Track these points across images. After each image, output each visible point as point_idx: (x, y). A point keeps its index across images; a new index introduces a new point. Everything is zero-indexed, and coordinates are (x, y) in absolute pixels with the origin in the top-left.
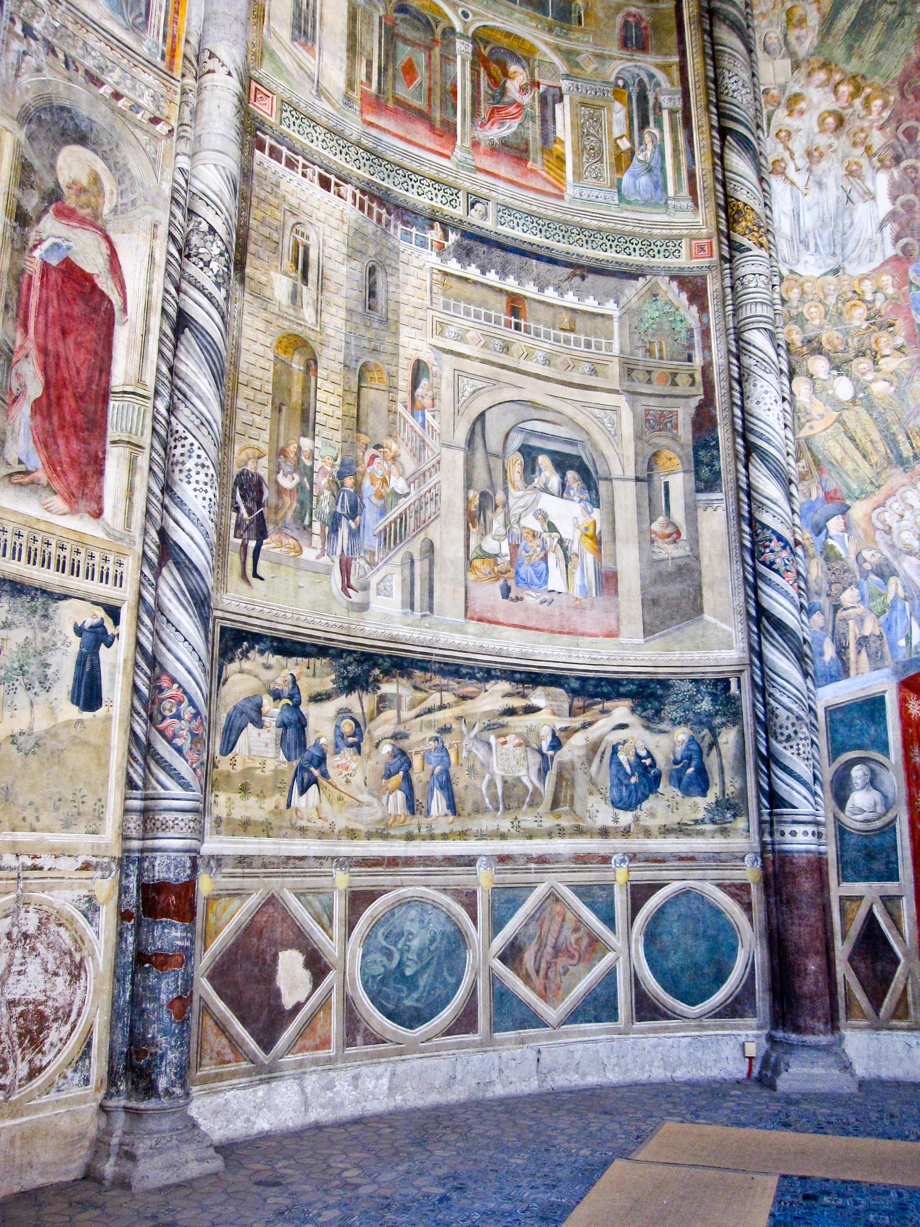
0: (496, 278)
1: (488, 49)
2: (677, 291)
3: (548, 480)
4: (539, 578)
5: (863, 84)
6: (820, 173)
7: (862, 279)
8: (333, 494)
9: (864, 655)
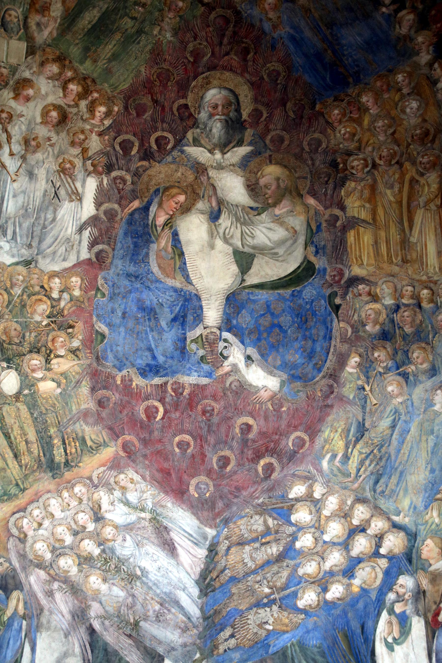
5: (92, 88)
6: (33, 163)
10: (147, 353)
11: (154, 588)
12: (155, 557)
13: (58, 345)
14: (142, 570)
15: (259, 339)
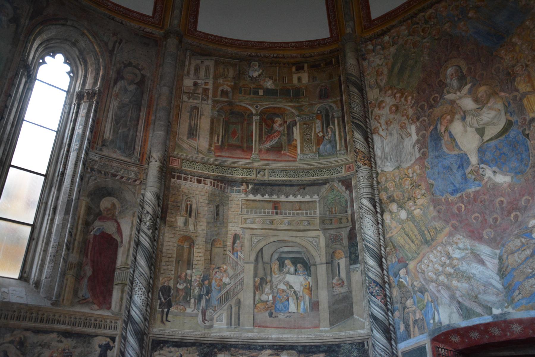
0: (268, 197)
1: (266, 116)
2: (341, 186)
3: (289, 269)
4: (285, 308)
7: (408, 168)
8: (200, 288)
9: (416, 328)
10: (452, 185)
11: (480, 280)
12: (477, 268)
13: (417, 194)
14: (473, 274)
15: (496, 162)
